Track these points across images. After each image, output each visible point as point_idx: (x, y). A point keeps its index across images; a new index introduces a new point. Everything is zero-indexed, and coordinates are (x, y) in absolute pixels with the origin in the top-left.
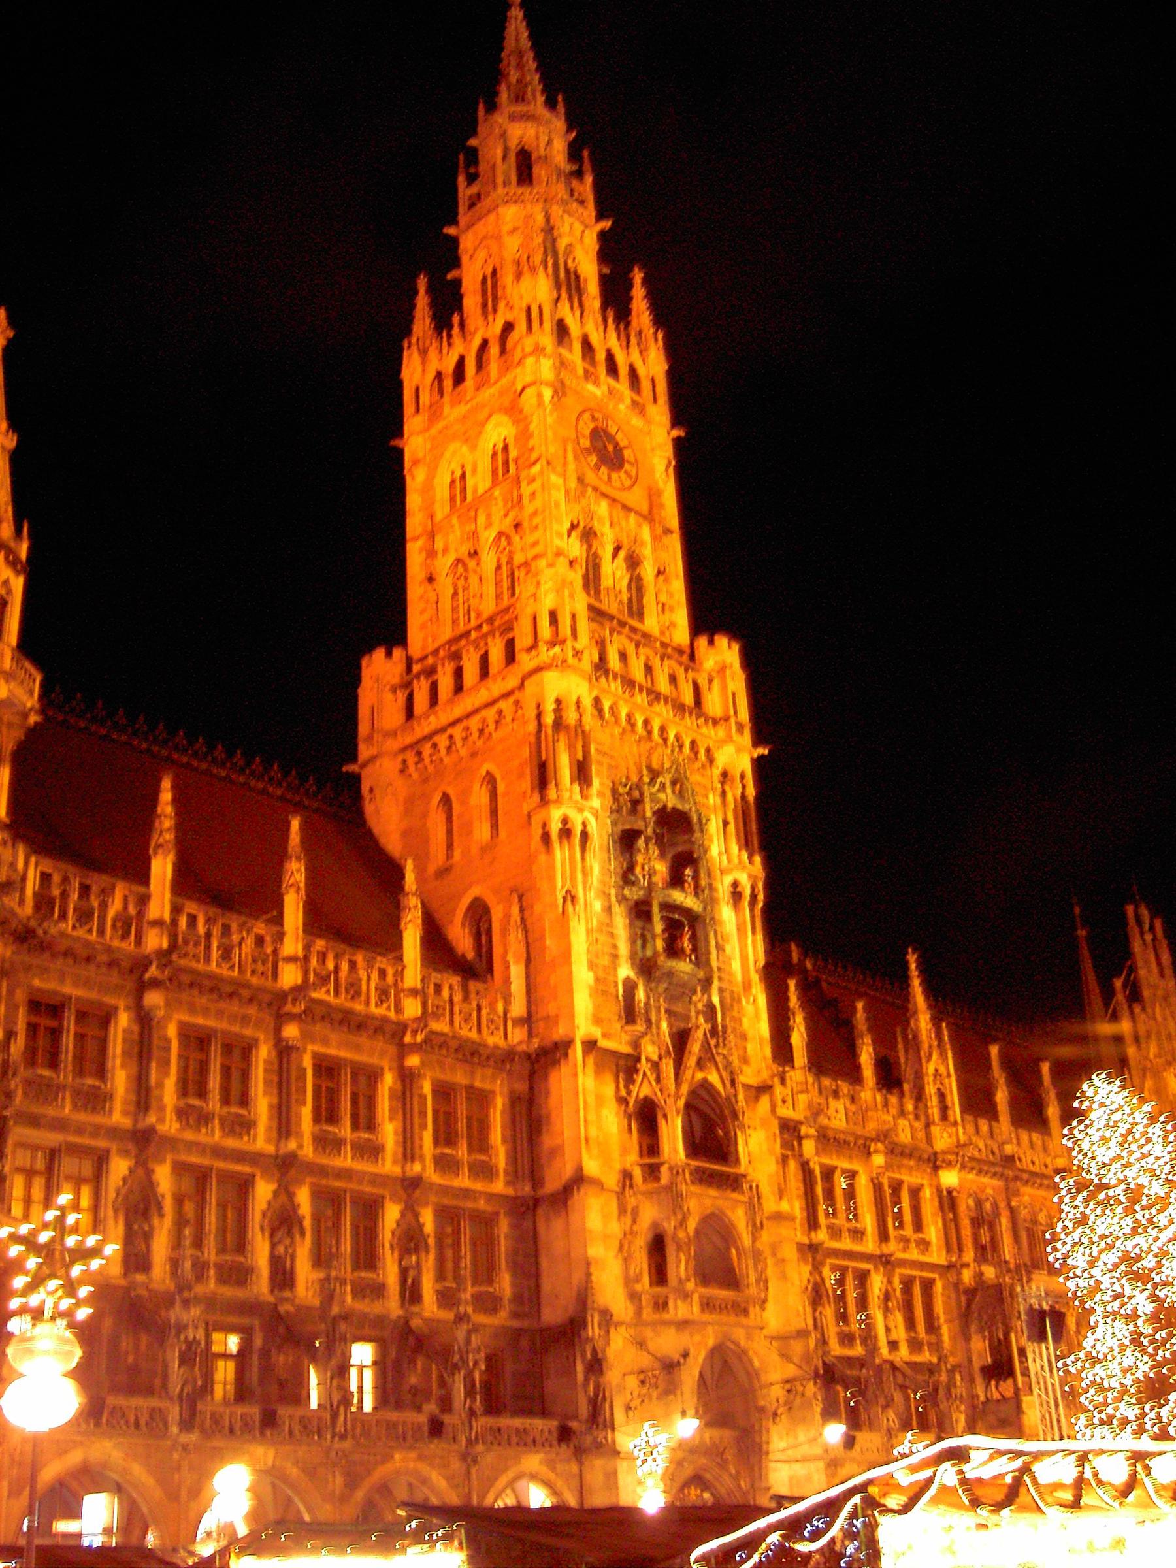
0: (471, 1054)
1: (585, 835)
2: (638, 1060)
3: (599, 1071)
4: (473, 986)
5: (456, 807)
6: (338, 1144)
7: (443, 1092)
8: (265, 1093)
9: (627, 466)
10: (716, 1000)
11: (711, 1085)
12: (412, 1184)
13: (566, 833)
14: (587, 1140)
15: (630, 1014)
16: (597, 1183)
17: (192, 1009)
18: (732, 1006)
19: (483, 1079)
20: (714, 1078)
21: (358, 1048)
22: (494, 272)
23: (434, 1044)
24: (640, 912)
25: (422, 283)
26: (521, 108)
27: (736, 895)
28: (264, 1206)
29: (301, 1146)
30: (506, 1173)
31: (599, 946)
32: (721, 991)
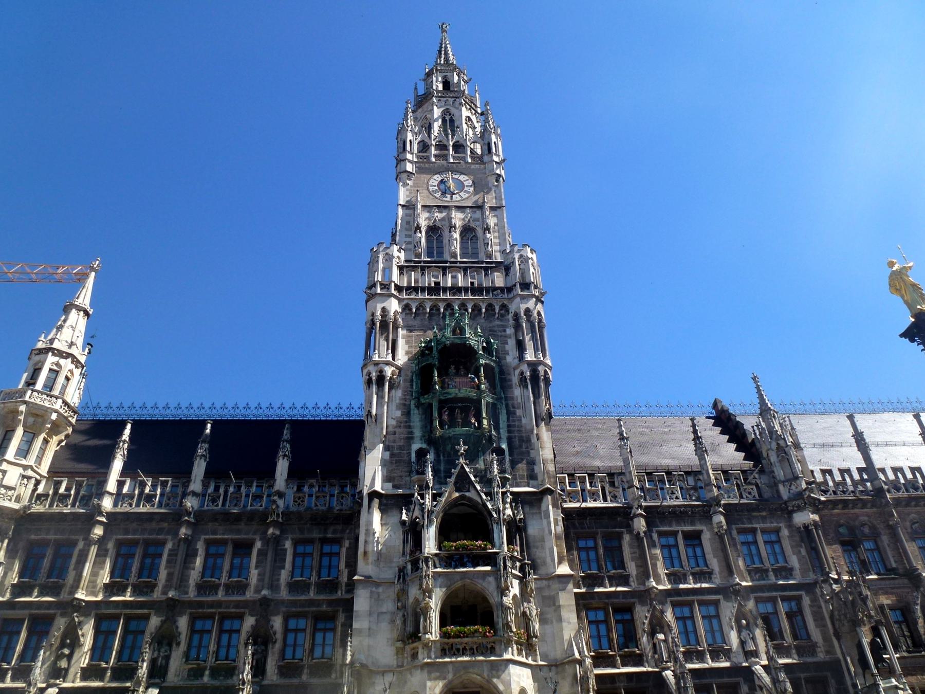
2: (413, 495)
6: (214, 588)
8: (166, 567)
9: (466, 189)
10: (504, 446)
11: (470, 499)
14: (365, 553)
17: (126, 532)
18: (521, 446)
19: (334, 532)
20: (471, 494)
21: (239, 532)
27: (523, 380)
28: (153, 630)
29: (187, 593)
30: (347, 585)
31: (397, 436)
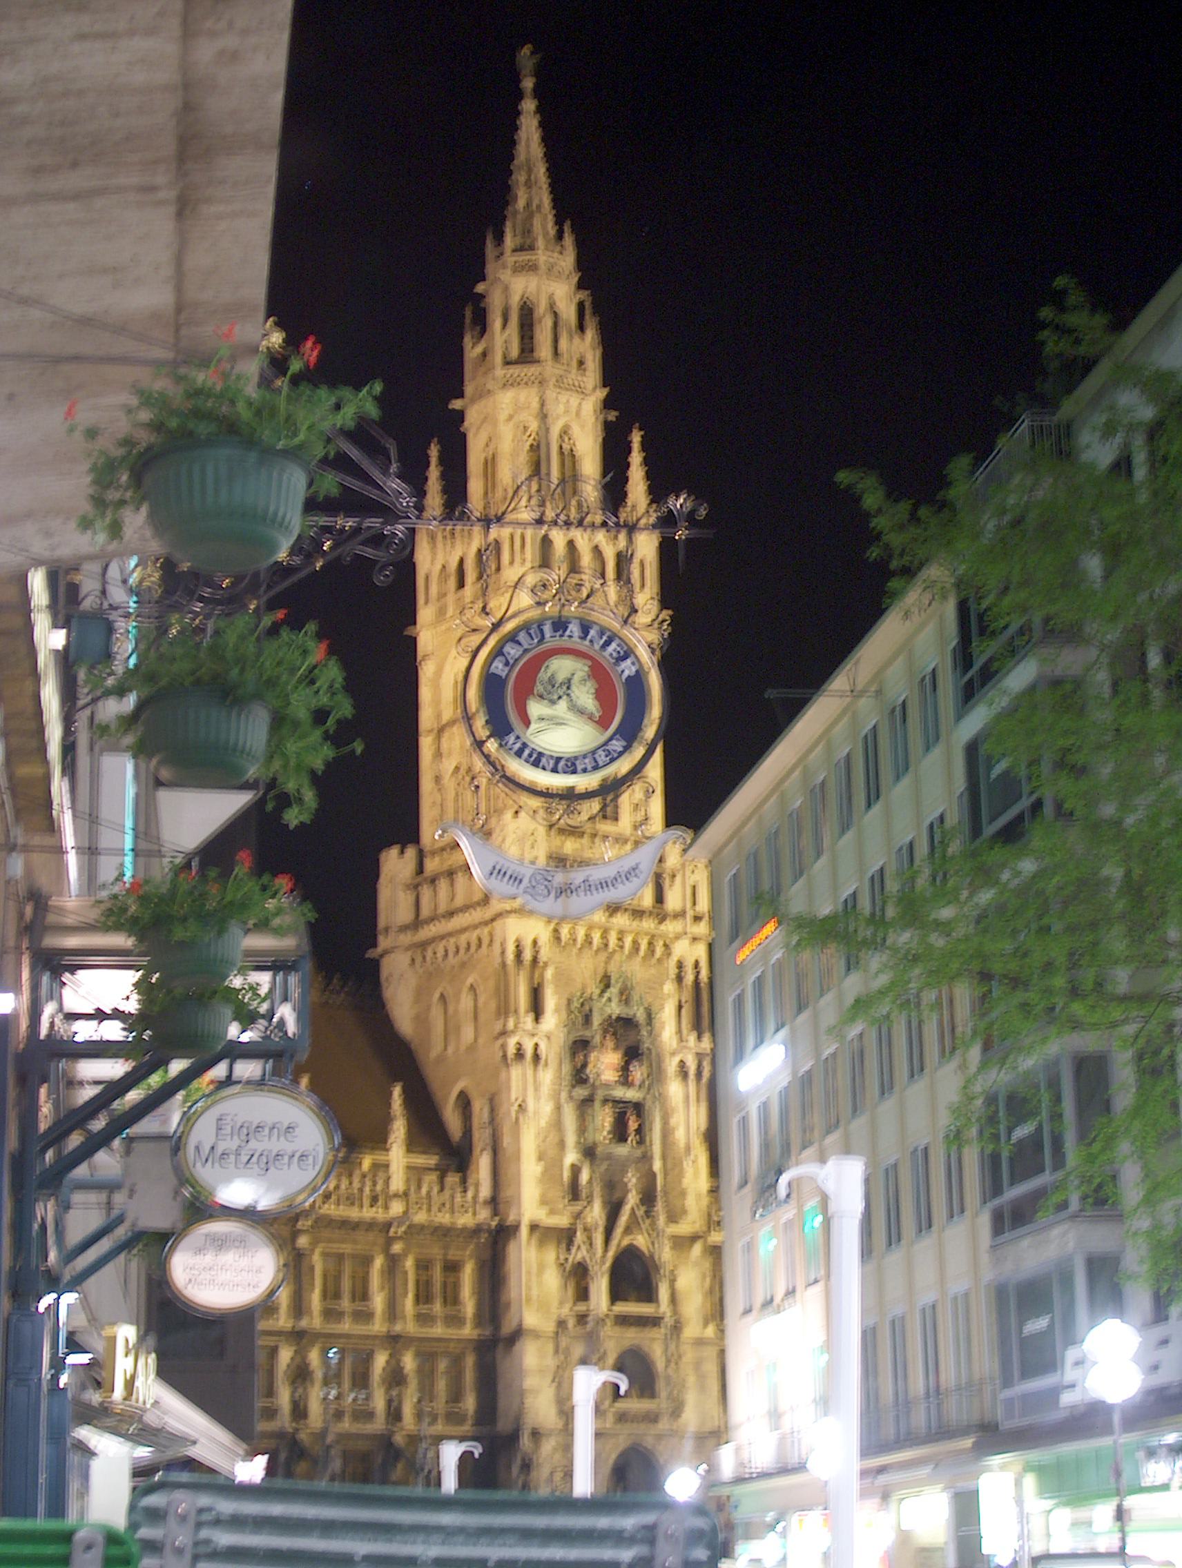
0: (444, 1233)
1: (536, 1057)
3: (542, 1243)
4: (452, 1179)
5: (451, 1009)
7: (423, 1266)
12: (394, 1341)
13: (520, 1055)
15: (574, 1191)
16: (536, 1334)
22: (493, 458)
23: (414, 1231)
24: (585, 1104)
25: (434, 452)
26: (524, 257)
32: (664, 1158)
